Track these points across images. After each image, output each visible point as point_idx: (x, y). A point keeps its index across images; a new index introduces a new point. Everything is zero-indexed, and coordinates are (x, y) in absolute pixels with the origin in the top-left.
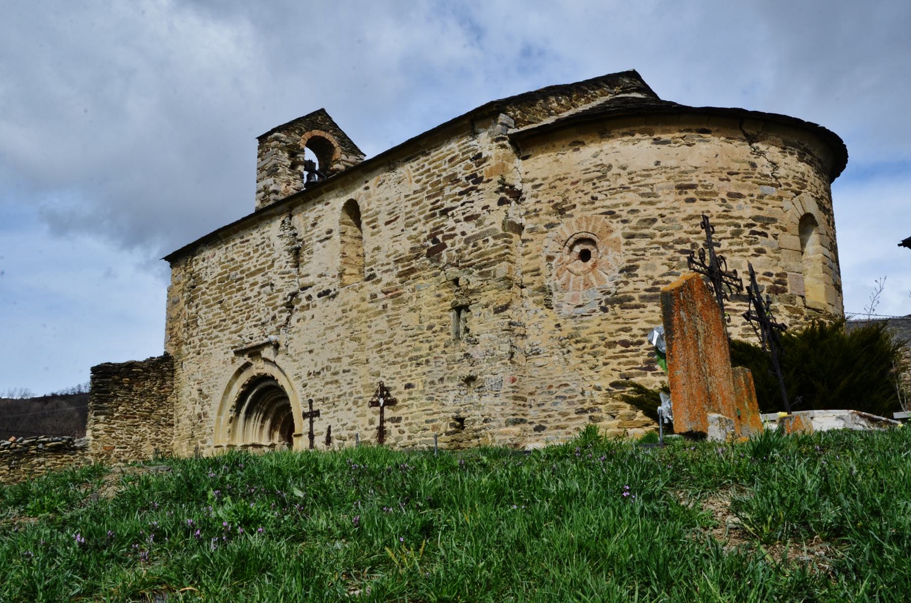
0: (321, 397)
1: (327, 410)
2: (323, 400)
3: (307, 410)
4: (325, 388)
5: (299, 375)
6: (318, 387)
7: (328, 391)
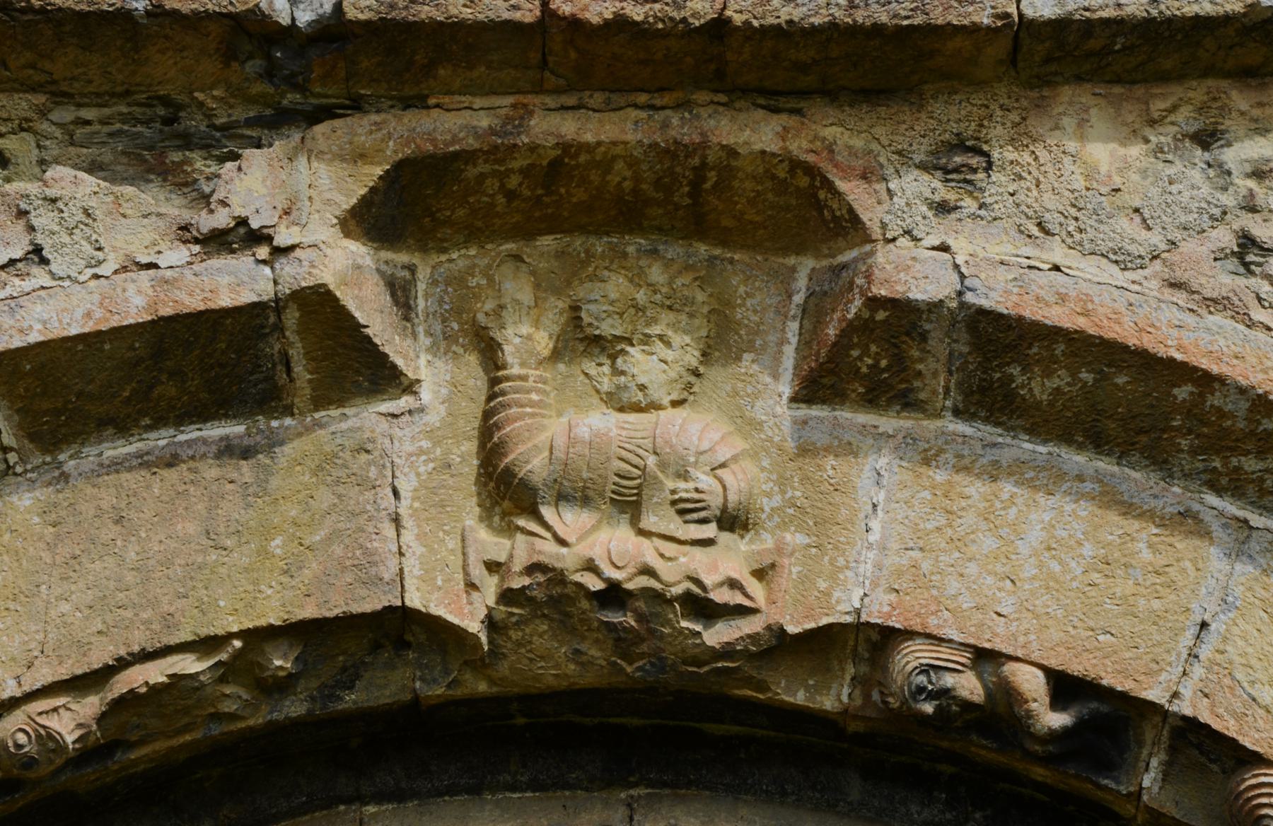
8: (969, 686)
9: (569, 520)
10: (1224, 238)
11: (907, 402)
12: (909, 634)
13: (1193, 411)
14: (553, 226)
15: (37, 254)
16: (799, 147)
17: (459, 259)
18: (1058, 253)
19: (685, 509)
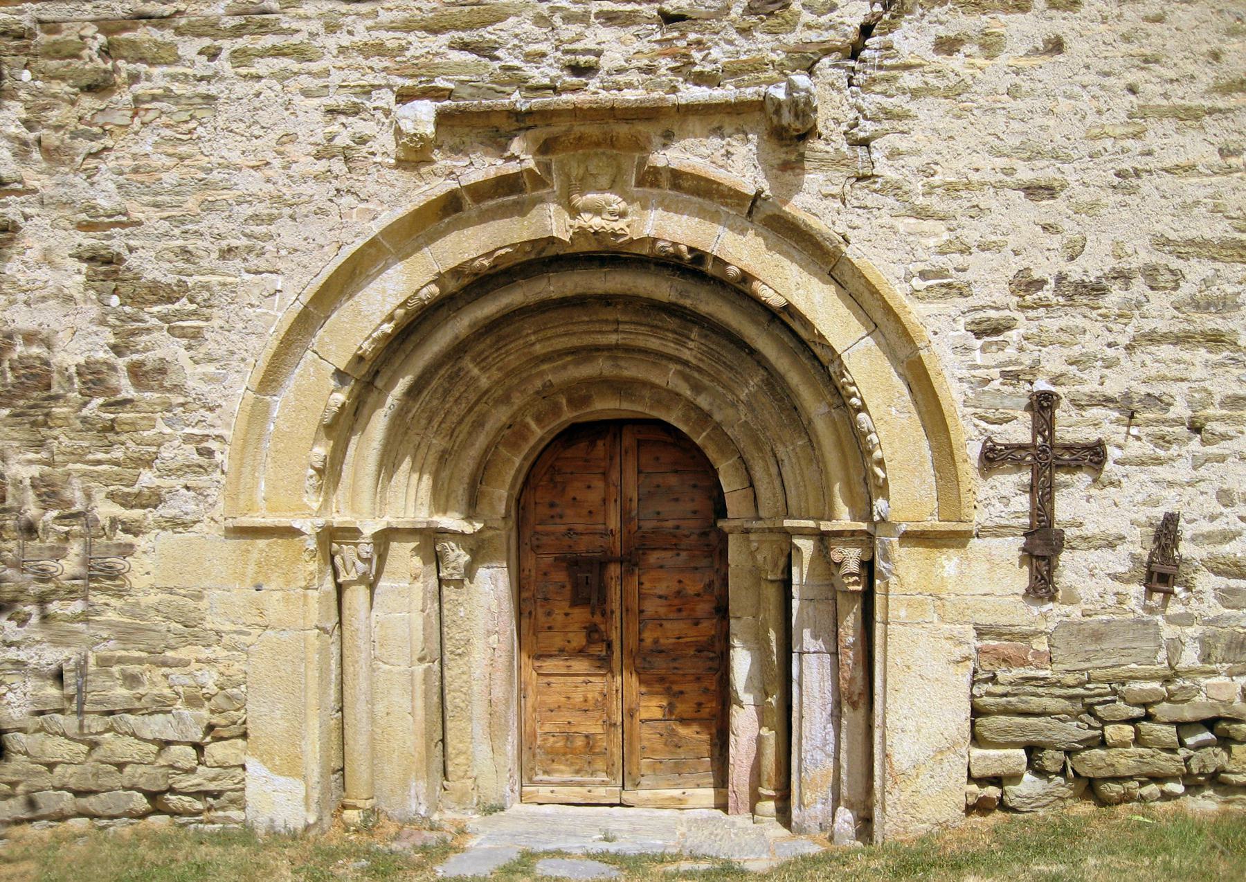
0: (1113, 388)
1: (1148, 449)
2: (1128, 409)
3: (1020, 431)
4: (1138, 356)
5: (957, 279)
6: (1091, 344)
7: (1153, 369)
8: (671, 250)
9: (586, 216)
10: (723, 151)
11: (658, 186)
12: (658, 239)
13: (717, 190)
14: (581, 148)
15: (471, 163)
16: (633, 131)
17: (561, 156)
18: (689, 155)
19: (611, 214)
